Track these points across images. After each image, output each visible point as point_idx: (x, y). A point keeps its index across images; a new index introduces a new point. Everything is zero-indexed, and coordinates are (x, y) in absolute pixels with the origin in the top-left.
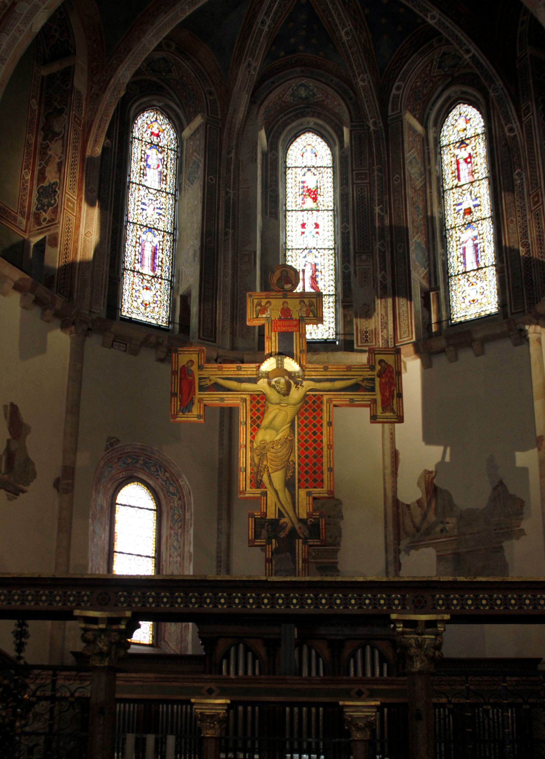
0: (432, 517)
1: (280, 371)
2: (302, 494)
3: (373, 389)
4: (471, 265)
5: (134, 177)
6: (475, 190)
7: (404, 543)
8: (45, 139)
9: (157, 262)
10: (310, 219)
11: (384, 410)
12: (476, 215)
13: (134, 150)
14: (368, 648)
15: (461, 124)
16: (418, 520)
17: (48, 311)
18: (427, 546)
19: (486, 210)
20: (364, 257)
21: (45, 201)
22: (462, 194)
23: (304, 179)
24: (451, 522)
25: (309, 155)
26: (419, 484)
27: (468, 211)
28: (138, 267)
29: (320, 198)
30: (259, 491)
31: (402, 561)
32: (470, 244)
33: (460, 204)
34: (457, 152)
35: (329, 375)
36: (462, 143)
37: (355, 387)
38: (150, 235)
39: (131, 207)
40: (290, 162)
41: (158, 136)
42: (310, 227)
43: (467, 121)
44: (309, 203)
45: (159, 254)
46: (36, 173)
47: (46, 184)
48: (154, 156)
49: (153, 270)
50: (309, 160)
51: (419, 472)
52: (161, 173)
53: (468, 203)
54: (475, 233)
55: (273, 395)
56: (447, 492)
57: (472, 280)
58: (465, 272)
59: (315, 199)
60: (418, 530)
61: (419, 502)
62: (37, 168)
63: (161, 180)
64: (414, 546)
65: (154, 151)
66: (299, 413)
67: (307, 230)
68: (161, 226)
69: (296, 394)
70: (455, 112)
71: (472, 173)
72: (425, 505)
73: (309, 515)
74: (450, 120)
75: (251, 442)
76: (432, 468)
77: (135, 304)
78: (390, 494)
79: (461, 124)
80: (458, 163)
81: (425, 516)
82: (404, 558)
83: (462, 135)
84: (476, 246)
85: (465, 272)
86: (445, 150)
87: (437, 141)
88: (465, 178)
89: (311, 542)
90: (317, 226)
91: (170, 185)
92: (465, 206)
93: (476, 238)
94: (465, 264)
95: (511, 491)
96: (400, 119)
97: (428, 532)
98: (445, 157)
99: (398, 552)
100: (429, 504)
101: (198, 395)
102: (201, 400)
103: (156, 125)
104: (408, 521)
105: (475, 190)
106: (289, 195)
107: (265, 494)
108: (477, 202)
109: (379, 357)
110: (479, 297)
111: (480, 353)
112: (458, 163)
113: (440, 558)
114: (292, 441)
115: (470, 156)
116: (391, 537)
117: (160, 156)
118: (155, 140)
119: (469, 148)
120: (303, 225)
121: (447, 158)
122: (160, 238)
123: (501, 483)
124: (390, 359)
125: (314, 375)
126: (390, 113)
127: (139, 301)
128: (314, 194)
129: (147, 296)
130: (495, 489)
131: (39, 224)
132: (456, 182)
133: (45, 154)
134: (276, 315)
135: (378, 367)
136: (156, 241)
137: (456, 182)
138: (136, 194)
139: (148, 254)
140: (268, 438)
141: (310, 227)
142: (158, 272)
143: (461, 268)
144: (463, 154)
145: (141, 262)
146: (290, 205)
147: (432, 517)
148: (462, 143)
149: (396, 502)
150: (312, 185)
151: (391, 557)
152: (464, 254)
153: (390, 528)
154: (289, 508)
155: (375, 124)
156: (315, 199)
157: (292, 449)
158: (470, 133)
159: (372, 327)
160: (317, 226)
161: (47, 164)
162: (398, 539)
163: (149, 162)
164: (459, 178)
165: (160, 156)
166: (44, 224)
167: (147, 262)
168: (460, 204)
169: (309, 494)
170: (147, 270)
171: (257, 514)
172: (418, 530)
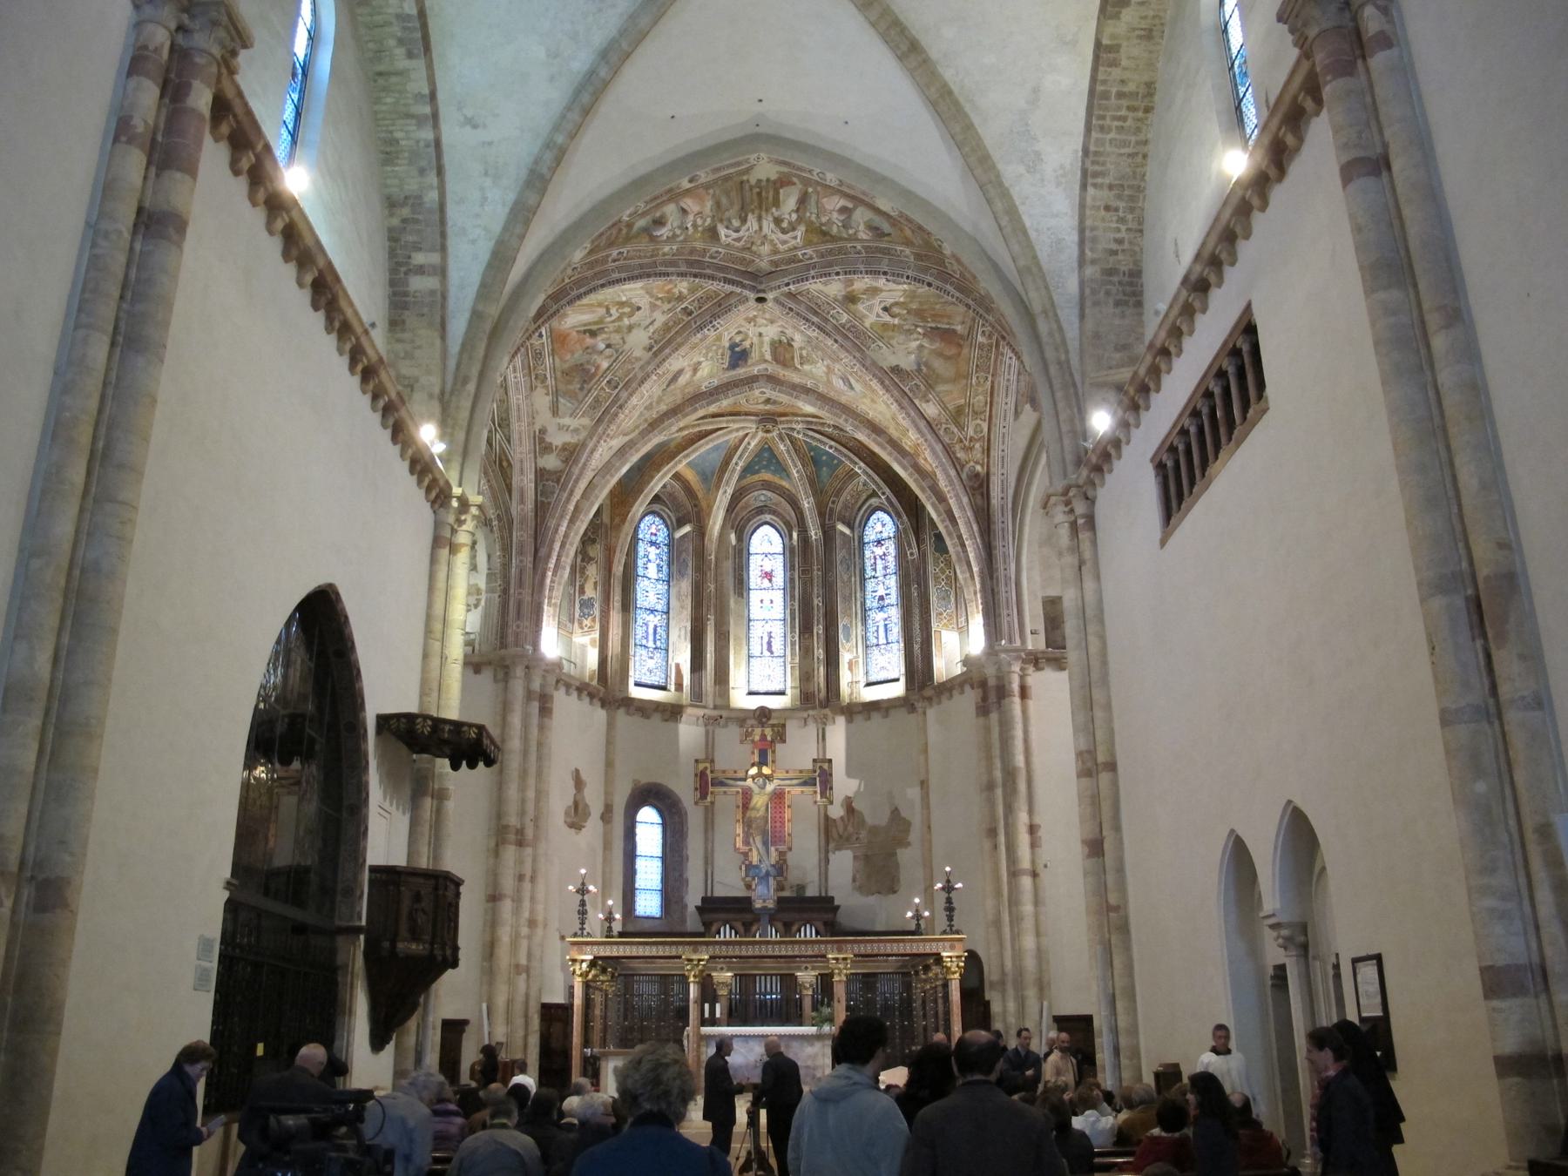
0: (850, 829)
1: (760, 774)
2: (772, 849)
3: (815, 785)
4: (882, 640)
5: (640, 571)
6: (887, 582)
7: (832, 846)
8: (583, 560)
9: (658, 637)
10: (767, 596)
11: (822, 797)
12: (887, 602)
13: (640, 549)
14: (808, 926)
15: (879, 527)
16: (841, 829)
17: (595, 700)
18: (847, 849)
19: (893, 598)
20: (806, 636)
21: (586, 611)
22: (877, 584)
23: (762, 563)
24: (863, 834)
25: (766, 544)
26: (842, 805)
27: (881, 598)
28: (644, 642)
29: (773, 579)
30: (747, 848)
31: (831, 858)
32: (881, 624)
33: (875, 591)
34: (875, 549)
35: (789, 776)
36: (879, 542)
37: (805, 784)
38: (652, 616)
39: (639, 595)
40: (752, 550)
41: (656, 535)
42: (766, 602)
43: (884, 525)
44: (766, 583)
45: (658, 629)
46: (577, 588)
47: (585, 597)
48: (653, 551)
49: (655, 643)
50: (767, 548)
51: (843, 797)
52: (658, 565)
53: (881, 592)
54: (886, 616)
55: (756, 789)
56: (861, 813)
57: (883, 651)
58: (877, 645)
59: (770, 580)
60: (841, 837)
61: (842, 818)
62: (578, 584)
63: (659, 571)
64: (839, 848)
65: (653, 548)
66: (771, 799)
67: (764, 605)
68: (659, 607)
69: (770, 787)
70: (874, 516)
71: (886, 568)
72: (846, 819)
73: (777, 862)
74: (871, 523)
75: (743, 818)
76: (851, 795)
77: (643, 671)
78: (822, 815)
79: (879, 527)
80: (875, 558)
81: (845, 829)
82: (832, 857)
83: (879, 536)
84: (886, 625)
85: (877, 645)
86: (867, 547)
87: (861, 538)
88: (880, 572)
89: (779, 878)
90: (772, 602)
91: (663, 576)
92: (879, 594)
93: (886, 619)
94: (877, 638)
95: (903, 814)
96: (834, 528)
97: (848, 839)
98: (866, 552)
99: (827, 852)
100: (849, 820)
101: (711, 789)
102: (712, 793)
103: (654, 526)
104: (834, 830)
105: (887, 582)
106: (751, 576)
107: (751, 850)
108: (888, 592)
109: (819, 764)
110: (886, 665)
111: (886, 716)
112: (875, 558)
113: (855, 858)
114: (767, 817)
115: (884, 554)
116: (823, 842)
117: (658, 551)
118: (654, 538)
119: (883, 547)
120: (762, 601)
121: (868, 553)
122: (659, 617)
123: (896, 809)
124: (826, 766)
125: (780, 776)
126: (827, 522)
127: (646, 668)
128: (769, 576)
129: (651, 664)
130: (892, 812)
131: (582, 628)
132: (873, 573)
133: (584, 573)
134: (757, 738)
135: (818, 771)
136: (656, 622)
137: (873, 573)
138: (641, 585)
139: (651, 631)
140: (753, 815)
141: (766, 602)
142: (658, 643)
143: (875, 641)
144: (879, 551)
145: (647, 638)
146: (752, 585)
147: (850, 829)
148: (879, 542)
149: (827, 818)
150: (768, 569)
151: (823, 856)
152: (877, 631)
153: (822, 836)
154: (765, 858)
155: (816, 534)
156: (770, 580)
157: (767, 822)
158: (885, 535)
159: (812, 690)
160: (772, 602)
161: (585, 580)
162: (827, 843)
163: (650, 557)
164: (875, 570)
165: (658, 551)
166: (586, 629)
167: (651, 637)
168: (875, 591)
169: (776, 850)
170: (651, 644)
171: (747, 862)
172: (841, 837)
